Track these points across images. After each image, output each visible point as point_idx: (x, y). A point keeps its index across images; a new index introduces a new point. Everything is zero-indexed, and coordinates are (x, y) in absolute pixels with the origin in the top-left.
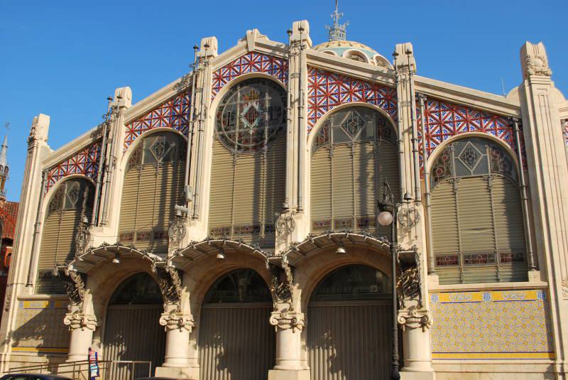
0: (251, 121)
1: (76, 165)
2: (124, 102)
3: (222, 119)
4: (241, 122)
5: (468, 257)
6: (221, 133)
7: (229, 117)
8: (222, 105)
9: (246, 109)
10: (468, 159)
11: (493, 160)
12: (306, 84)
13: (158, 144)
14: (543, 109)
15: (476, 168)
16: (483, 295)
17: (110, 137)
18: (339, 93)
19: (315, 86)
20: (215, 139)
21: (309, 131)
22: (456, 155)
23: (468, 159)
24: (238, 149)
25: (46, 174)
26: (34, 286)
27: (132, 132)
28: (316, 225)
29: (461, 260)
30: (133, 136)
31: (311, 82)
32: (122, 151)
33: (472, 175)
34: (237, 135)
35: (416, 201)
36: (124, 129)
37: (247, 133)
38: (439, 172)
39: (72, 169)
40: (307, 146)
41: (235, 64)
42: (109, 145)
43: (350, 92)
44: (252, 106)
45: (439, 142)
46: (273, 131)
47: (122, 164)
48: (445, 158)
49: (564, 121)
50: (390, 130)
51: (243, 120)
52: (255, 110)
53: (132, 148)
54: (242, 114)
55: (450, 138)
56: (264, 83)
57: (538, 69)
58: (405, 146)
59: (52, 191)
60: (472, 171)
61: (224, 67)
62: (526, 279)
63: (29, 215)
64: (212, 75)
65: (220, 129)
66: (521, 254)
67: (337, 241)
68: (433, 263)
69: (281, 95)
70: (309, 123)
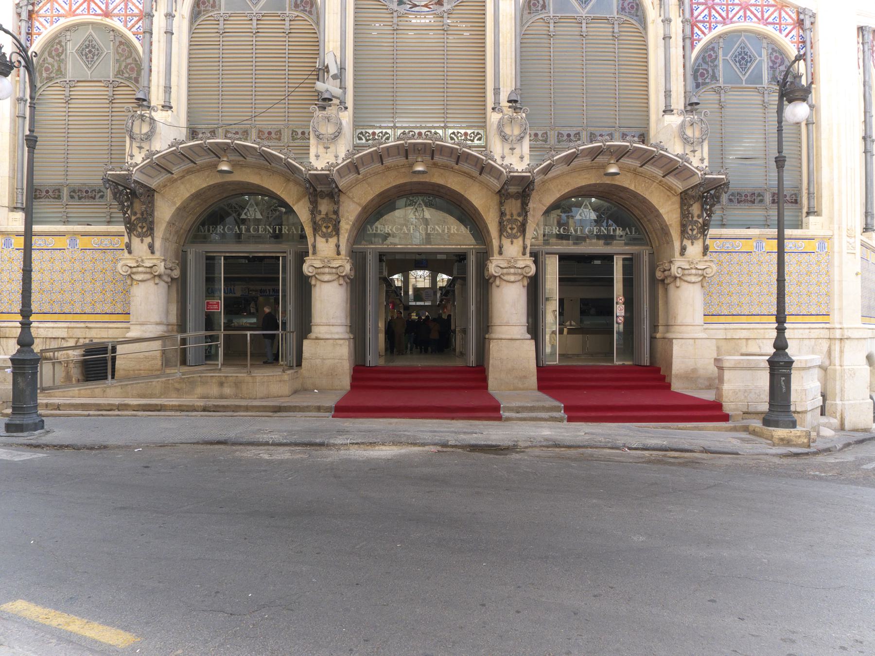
10: (740, 62)
11: (771, 67)
22: (725, 54)
24: (398, 5)
33: (744, 85)
38: (702, 75)
45: (706, 31)
48: (710, 56)
50: (637, 5)
60: (744, 79)
66: (795, 194)
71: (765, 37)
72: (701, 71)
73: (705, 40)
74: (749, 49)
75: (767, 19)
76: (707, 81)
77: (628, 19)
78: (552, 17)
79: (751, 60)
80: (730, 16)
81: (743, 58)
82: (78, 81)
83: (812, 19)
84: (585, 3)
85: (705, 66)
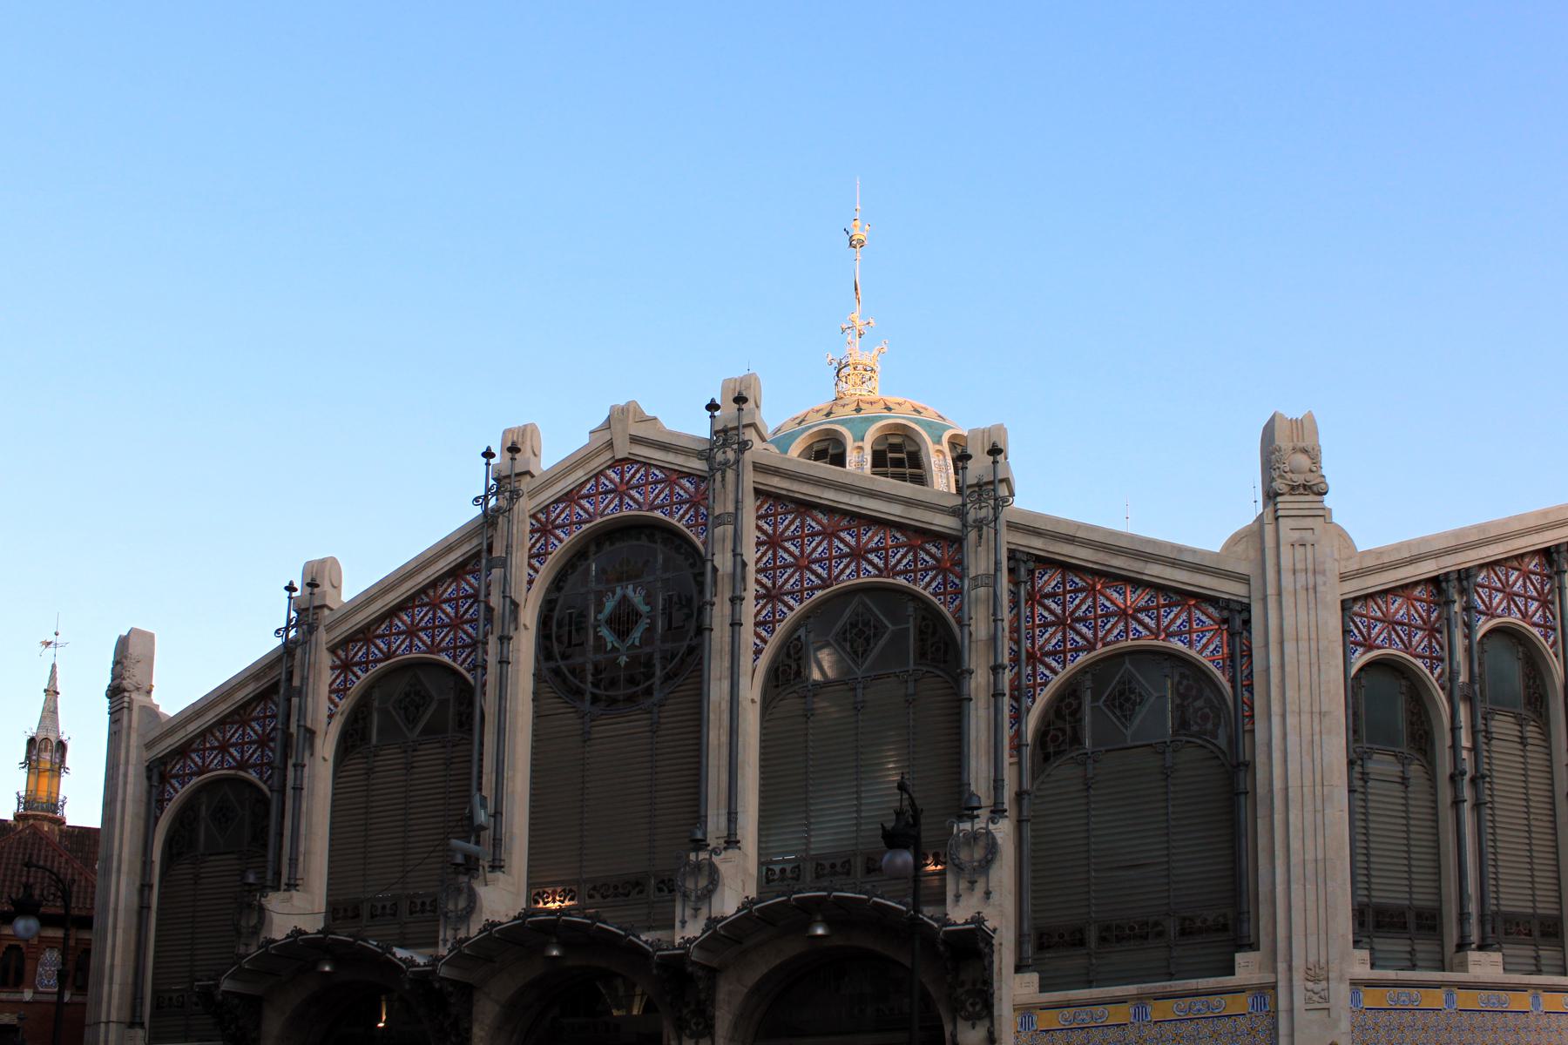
0: (622, 634)
1: (223, 748)
2: (324, 595)
3: (554, 628)
4: (598, 638)
6: (552, 664)
7: (570, 625)
8: (554, 596)
9: (610, 605)
10: (1121, 706)
11: (1178, 706)
12: (750, 535)
13: (407, 695)
16: (1132, 1011)
17: (296, 682)
18: (830, 559)
19: (772, 542)
20: (538, 677)
21: (758, 652)
22: (1095, 698)
23: (1121, 706)
25: (155, 771)
26: (147, 1024)
27: (345, 667)
28: (767, 877)
29: (1092, 935)
30: (351, 676)
31: (764, 532)
32: (326, 713)
33: (1129, 743)
35: (997, 812)
36: (326, 659)
37: (614, 663)
39: (214, 759)
40: (751, 690)
41: (584, 491)
42: (295, 701)
43: (857, 554)
44: (624, 597)
46: (673, 657)
47: (326, 746)
48: (1070, 705)
49: (1245, 615)
51: (604, 632)
53: (345, 704)
54: (600, 617)
55: (1083, 657)
56: (651, 538)
57: (1299, 479)
58: (978, 682)
59: (170, 809)
60: (1129, 733)
61: (557, 501)
63: (125, 868)
64: (528, 520)
67: (808, 910)
68: (1029, 949)
69: (693, 565)
70: (758, 635)
72: (1052, 733)
73: (1055, 682)
75: (1168, 626)
77: (931, 669)
78: (810, 687)
79: (1142, 700)
80: (1100, 634)
81: (1128, 699)
82: (211, 855)
83: (1245, 615)
84: (862, 656)
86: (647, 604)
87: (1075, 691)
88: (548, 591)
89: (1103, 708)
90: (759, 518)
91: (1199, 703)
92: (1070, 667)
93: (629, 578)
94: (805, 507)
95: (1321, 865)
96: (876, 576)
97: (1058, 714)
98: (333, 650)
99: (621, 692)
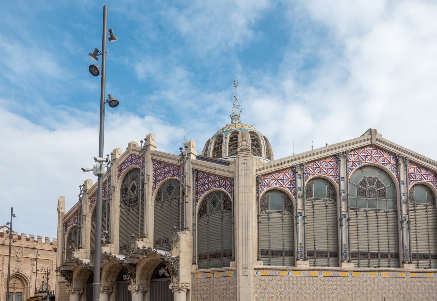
0: (133, 192)
4: (130, 193)
5: (211, 255)
6: (122, 199)
9: (131, 185)
14: (243, 171)
15: (217, 208)
19: (155, 170)
20: (121, 202)
22: (209, 202)
27: (92, 202)
33: (215, 212)
34: (128, 199)
52: (134, 185)
60: (215, 210)
62: (229, 266)
65: (122, 197)
71: (222, 192)
72: (202, 210)
74: (217, 198)
76: (203, 213)
81: (215, 202)
85: (203, 208)
86: (137, 185)
87: (205, 200)
88: (122, 183)
89: (210, 204)
90: (153, 165)
91: (228, 202)
92: (204, 194)
93: (134, 180)
94: (160, 162)
95: (246, 241)
96: (172, 176)
97: (203, 206)
98: (90, 198)
99: (133, 204)
